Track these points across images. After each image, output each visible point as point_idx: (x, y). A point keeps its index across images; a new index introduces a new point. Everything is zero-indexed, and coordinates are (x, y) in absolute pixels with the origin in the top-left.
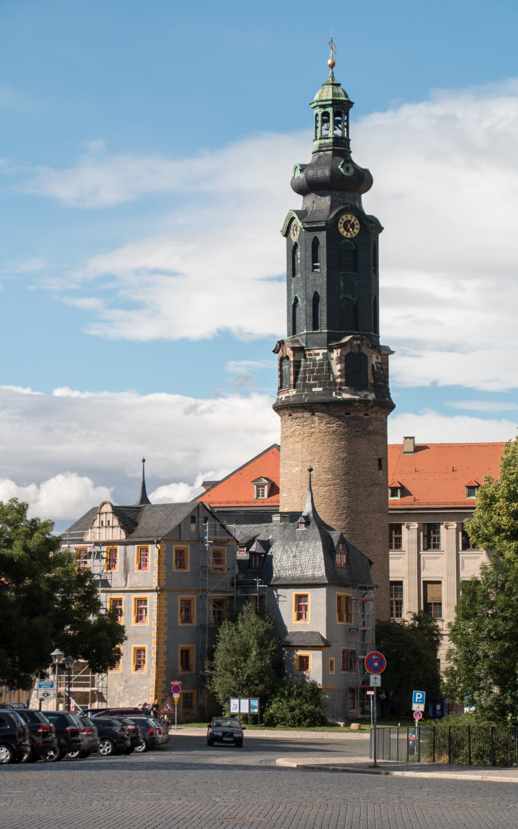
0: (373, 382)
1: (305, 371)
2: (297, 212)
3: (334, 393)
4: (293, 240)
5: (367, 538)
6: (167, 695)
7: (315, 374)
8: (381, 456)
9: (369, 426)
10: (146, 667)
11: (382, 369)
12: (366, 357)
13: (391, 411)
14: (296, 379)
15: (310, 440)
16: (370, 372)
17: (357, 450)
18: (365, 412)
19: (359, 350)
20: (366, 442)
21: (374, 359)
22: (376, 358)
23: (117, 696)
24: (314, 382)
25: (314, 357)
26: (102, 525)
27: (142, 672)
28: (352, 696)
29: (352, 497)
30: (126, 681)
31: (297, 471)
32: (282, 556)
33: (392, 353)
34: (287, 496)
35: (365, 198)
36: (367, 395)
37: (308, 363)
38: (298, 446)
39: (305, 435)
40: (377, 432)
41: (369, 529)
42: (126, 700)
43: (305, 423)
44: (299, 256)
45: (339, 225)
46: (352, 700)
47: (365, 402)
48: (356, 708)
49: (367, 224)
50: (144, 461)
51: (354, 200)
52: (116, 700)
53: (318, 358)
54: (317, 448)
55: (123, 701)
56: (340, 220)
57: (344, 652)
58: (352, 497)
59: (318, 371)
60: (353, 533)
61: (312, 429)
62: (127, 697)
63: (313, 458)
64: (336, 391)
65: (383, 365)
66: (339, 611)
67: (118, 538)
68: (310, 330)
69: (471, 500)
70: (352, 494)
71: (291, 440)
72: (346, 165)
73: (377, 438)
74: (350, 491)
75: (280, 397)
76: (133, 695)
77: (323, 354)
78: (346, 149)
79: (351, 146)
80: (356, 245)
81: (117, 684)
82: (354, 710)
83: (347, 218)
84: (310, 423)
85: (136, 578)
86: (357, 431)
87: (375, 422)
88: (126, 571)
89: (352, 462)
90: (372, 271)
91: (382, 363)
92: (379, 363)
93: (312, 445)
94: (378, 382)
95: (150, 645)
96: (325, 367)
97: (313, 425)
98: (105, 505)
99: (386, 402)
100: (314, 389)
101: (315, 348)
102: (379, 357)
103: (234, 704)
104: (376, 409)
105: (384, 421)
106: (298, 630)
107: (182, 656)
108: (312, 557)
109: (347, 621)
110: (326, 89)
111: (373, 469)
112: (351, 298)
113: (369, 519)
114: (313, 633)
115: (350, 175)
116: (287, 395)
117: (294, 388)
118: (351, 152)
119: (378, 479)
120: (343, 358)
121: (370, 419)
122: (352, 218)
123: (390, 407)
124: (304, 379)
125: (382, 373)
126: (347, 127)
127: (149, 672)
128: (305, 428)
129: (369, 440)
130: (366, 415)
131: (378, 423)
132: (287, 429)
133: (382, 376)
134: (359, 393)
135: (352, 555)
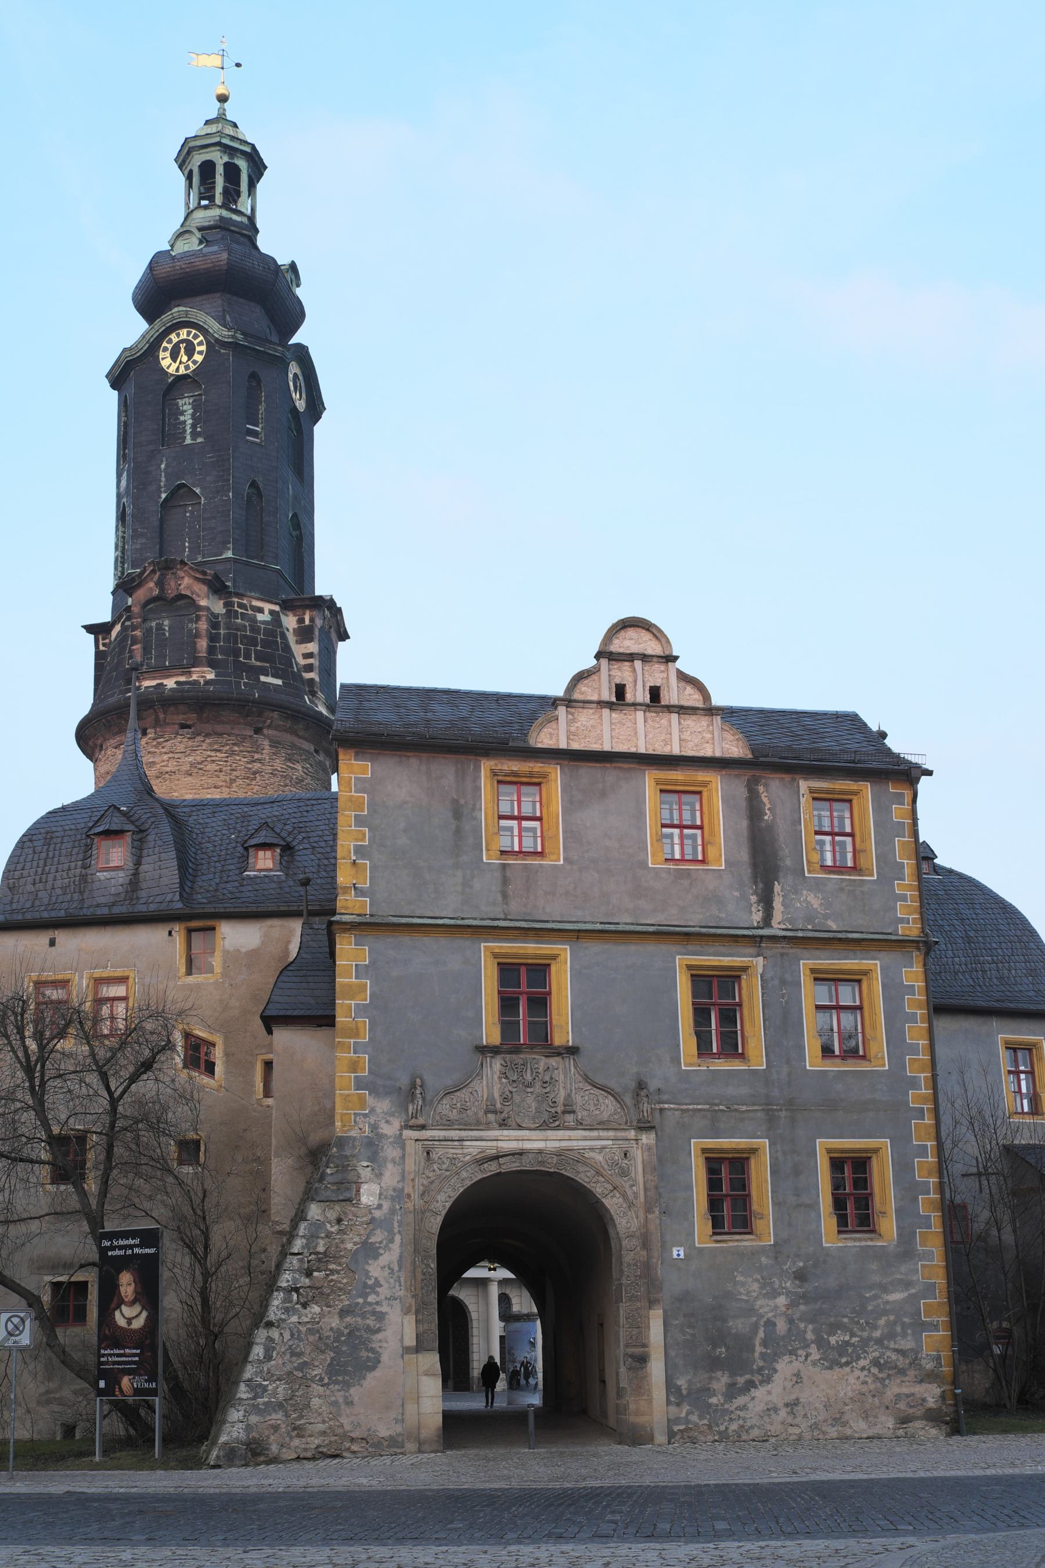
14: (211, 650)
15: (250, 787)
23: (761, 1334)
24: (258, 663)
25: (250, 612)
27: (872, 1240)
30: (800, 1276)
37: (239, 621)
42: (808, 1346)
43: (236, 748)
52: (759, 1349)
55: (792, 1353)
59: (265, 644)
61: (255, 764)
62: (810, 1336)
68: (242, 556)
76: (833, 1328)
81: (755, 1286)
84: (249, 749)
95: (901, 1140)
100: (263, 678)
127: (906, 1237)
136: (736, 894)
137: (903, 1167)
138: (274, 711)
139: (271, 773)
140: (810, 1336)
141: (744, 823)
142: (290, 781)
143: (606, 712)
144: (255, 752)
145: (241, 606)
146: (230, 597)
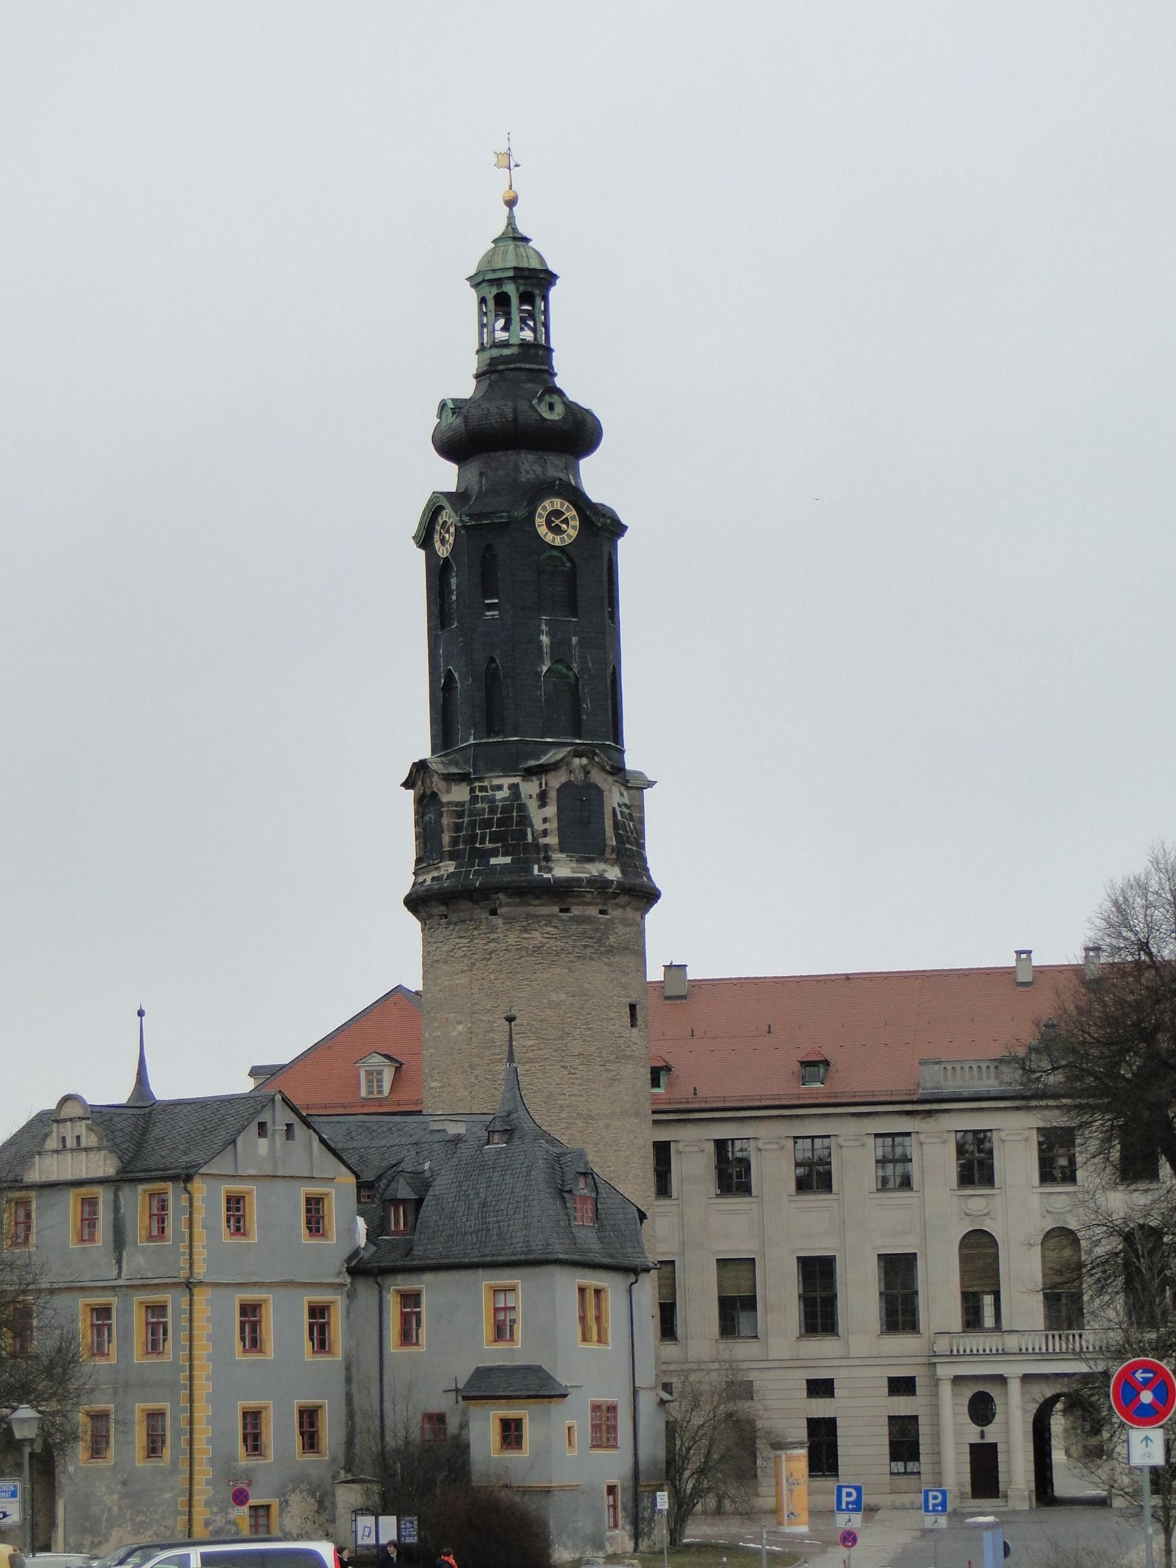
0: (615, 843)
1: (472, 824)
2: (447, 495)
3: (536, 867)
4: (440, 554)
5: (611, 1169)
6: (215, 1510)
7: (494, 829)
9: (610, 936)
10: (167, 1452)
11: (631, 818)
12: (600, 792)
13: (652, 906)
14: (455, 841)
16: (609, 823)
17: (586, 986)
18: (601, 907)
19: (585, 776)
20: (605, 967)
21: (615, 797)
22: (619, 794)
23: (106, 1515)
25: (490, 793)
26: (64, 1146)
27: (158, 1462)
28: (611, 1502)
29: (579, 1085)
31: (460, 1033)
32: (456, 1204)
33: (651, 784)
34: (440, 1088)
35: (587, 466)
36: (605, 871)
37: (479, 805)
38: (461, 980)
39: (476, 957)
40: (625, 948)
41: (615, 1151)
43: (476, 932)
44: (454, 587)
45: (538, 521)
46: (611, 1510)
47: (600, 885)
48: (620, 1527)
49: (594, 519)
50: (141, 1013)
51: (565, 471)
52: (104, 1524)
53: (499, 795)
54: (502, 983)
55: (120, 1526)
56: (539, 510)
57: (596, 1408)
58: (579, 1085)
59: (501, 822)
61: (491, 944)
62: (128, 1517)
63: (496, 1005)
64: (538, 862)
65: (632, 809)
66: (583, 1319)
67: (100, 1173)
69: (812, 1089)
71: (446, 967)
72: (547, 398)
74: (573, 1071)
75: (421, 879)
77: (511, 787)
78: (546, 368)
79: (554, 363)
80: (571, 561)
81: (104, 1489)
82: (617, 1532)
83: (553, 507)
84: (485, 931)
85: (141, 1259)
86: (585, 947)
87: (621, 926)
88: (119, 1242)
89: (576, 1012)
90: (607, 615)
91: (631, 805)
92: (626, 806)
93: (492, 977)
94: (625, 844)
96: (515, 814)
97: (493, 936)
98: (67, 1104)
99: (642, 885)
100: (493, 861)
101: (493, 774)
102: (625, 793)
103: (365, 1527)
104: (623, 899)
105: (639, 926)
106: (497, 1364)
107: (245, 1428)
108: (522, 1206)
109: (600, 1341)
110: (502, 248)
111: (620, 1026)
112: (565, 671)
113: (615, 1131)
114: (529, 1368)
115: (558, 419)
116: (435, 874)
117: (453, 856)
118: (555, 375)
119: (629, 1047)
120: (553, 795)
121: (612, 921)
122: (562, 505)
123: (650, 896)
124: (472, 839)
125: (632, 826)
126: (546, 325)
127: (175, 1461)
128: (477, 941)
129: (610, 965)
130: (602, 912)
131: (628, 929)
132: (436, 945)
133: (632, 833)
134: (588, 866)
135: (604, 1198)
136: (106, 1260)
137: (175, 1419)
138: (497, 893)
139: (506, 950)
140: (128, 1517)
141: (112, 1216)
142: (527, 952)
143: (55, 1155)
144: (490, 933)
145: (482, 789)
146: (472, 783)
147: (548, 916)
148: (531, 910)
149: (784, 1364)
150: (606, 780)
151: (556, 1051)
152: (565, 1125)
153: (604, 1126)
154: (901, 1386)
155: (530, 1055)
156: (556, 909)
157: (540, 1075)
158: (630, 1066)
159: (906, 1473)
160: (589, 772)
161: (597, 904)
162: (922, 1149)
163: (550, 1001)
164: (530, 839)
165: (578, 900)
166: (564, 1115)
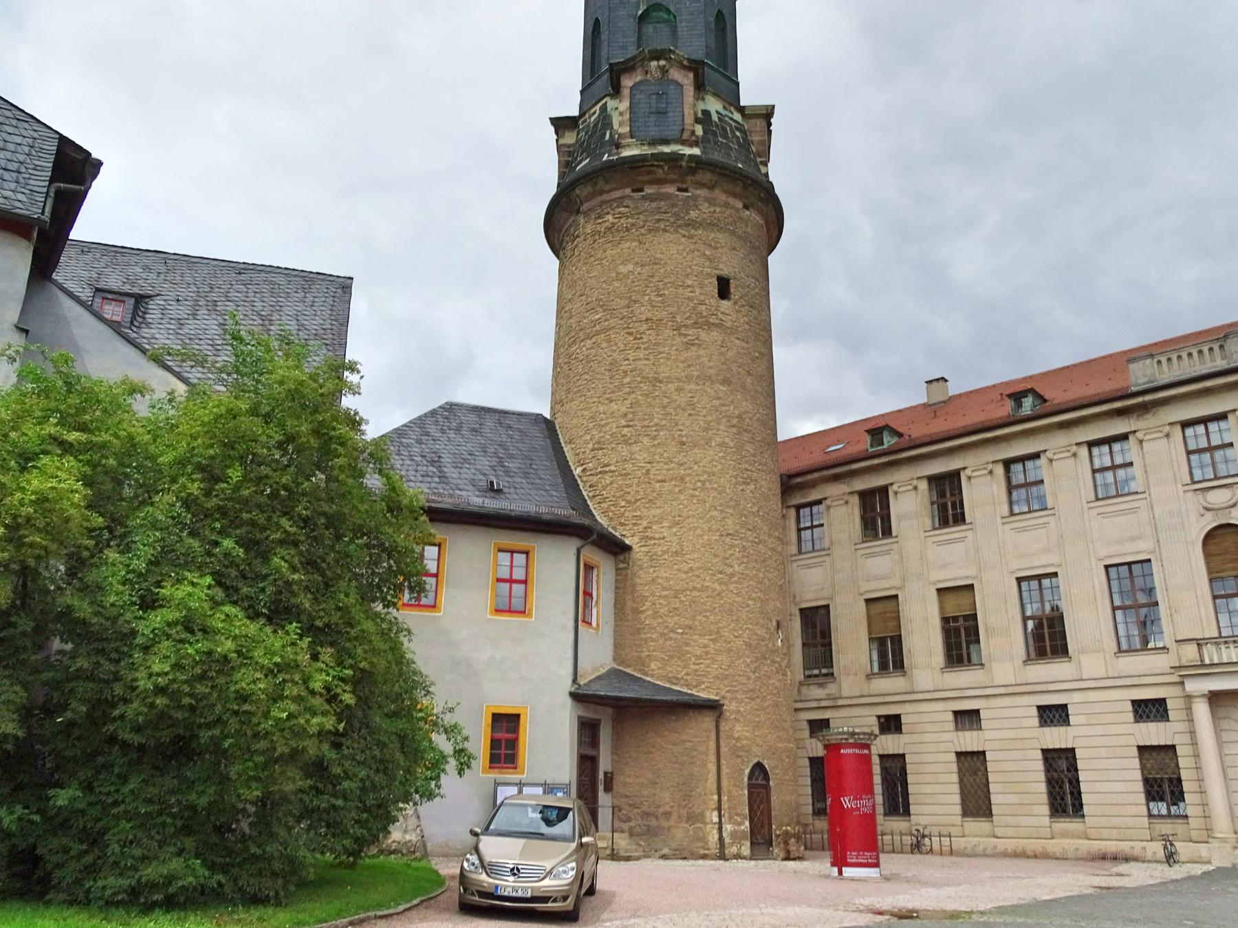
5: (684, 433)
8: (725, 272)
17: (659, 256)
18: (679, 185)
20: (683, 240)
29: (645, 349)
40: (715, 225)
41: (690, 415)
47: (674, 158)
58: (645, 349)
60: (645, 423)
70: (643, 343)
73: (712, 236)
86: (658, 221)
87: (707, 205)
104: (707, 177)
121: (695, 198)
129: (691, 237)
130: (679, 190)
147: (619, 198)
148: (606, 197)
149: (1010, 690)
150: (685, 76)
151: (622, 319)
152: (628, 390)
153: (676, 390)
154: (1151, 710)
155: (598, 327)
156: (628, 191)
157: (604, 345)
158: (715, 333)
159: (1169, 816)
160: (667, 71)
161: (672, 182)
162: (1142, 448)
163: (618, 274)
164: (607, 137)
165: (647, 178)
166: (627, 380)
